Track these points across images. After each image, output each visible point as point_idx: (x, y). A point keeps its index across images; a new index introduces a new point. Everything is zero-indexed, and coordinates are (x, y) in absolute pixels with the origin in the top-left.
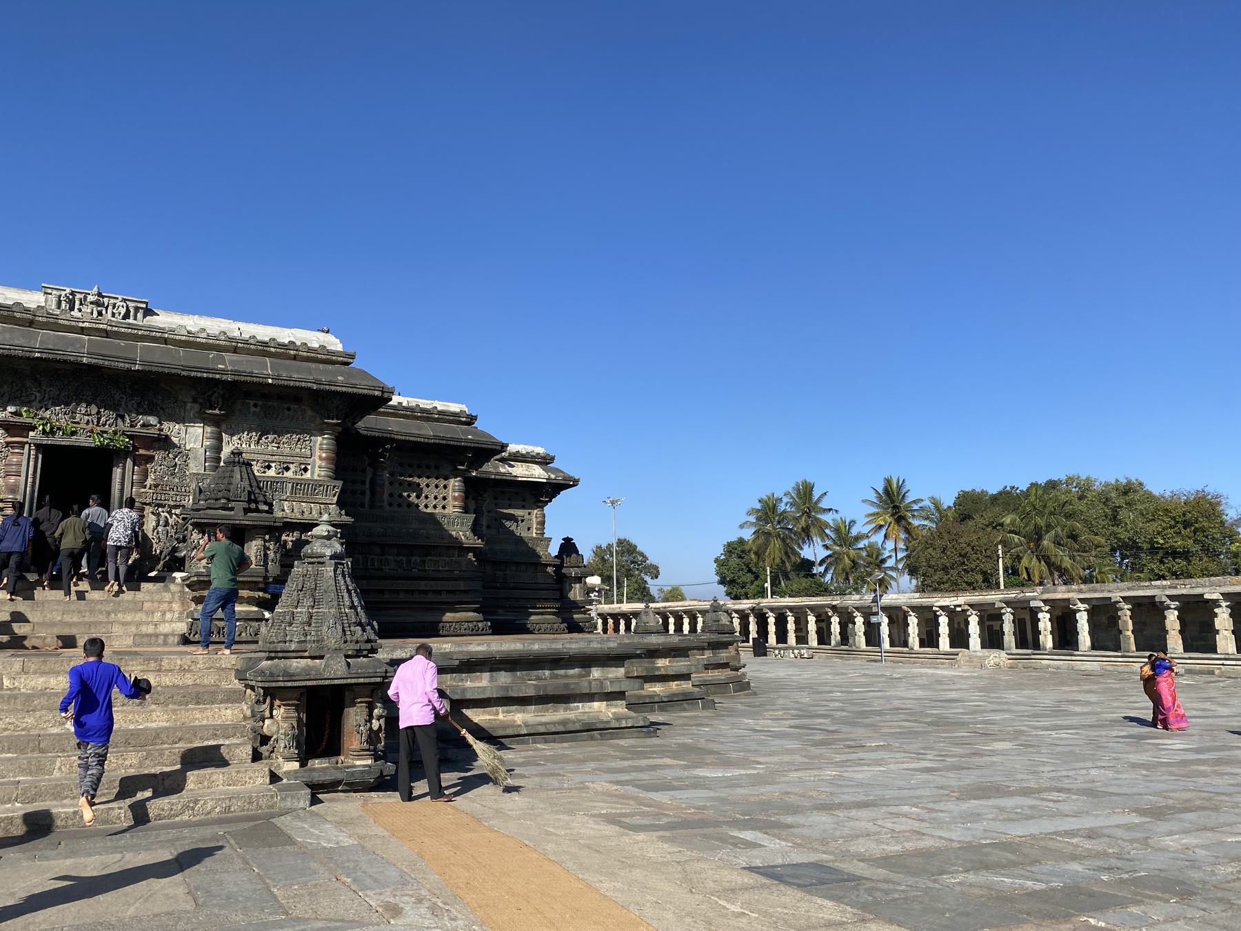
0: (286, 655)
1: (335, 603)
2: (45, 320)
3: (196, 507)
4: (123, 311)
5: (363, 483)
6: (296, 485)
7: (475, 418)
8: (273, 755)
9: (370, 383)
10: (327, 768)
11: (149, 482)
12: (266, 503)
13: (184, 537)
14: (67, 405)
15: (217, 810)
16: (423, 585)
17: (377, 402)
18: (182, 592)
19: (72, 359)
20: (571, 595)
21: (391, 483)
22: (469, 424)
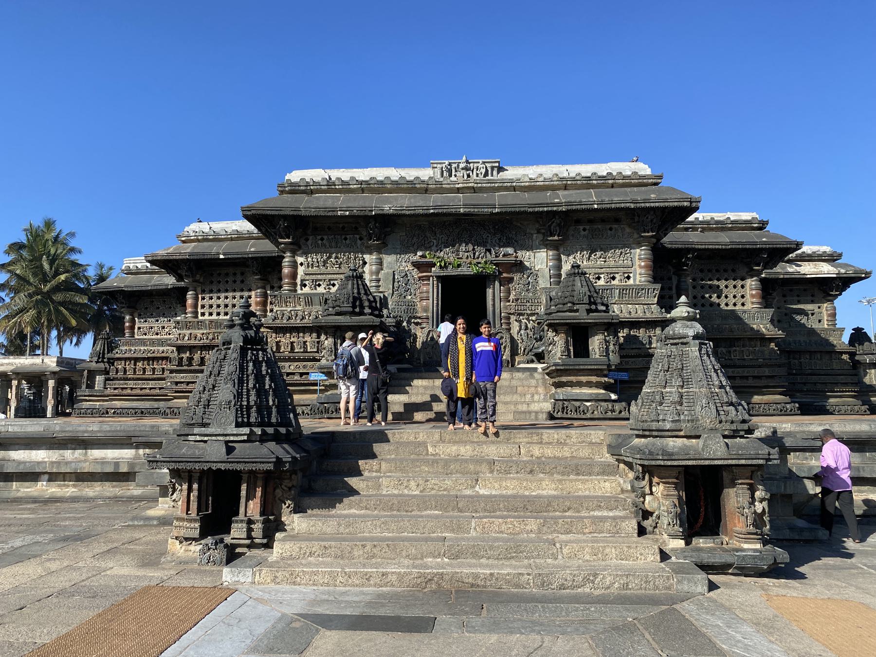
0: (660, 433)
1: (705, 383)
2: (434, 186)
3: (549, 311)
4: (483, 171)
5: (670, 289)
6: (623, 290)
7: (767, 223)
8: (657, 530)
9: (679, 196)
10: (714, 549)
11: (512, 297)
12: (603, 304)
13: (540, 337)
14: (453, 246)
15: (616, 585)
18: (543, 379)
19: (453, 210)
20: (867, 380)
21: (694, 287)
22: (760, 229)
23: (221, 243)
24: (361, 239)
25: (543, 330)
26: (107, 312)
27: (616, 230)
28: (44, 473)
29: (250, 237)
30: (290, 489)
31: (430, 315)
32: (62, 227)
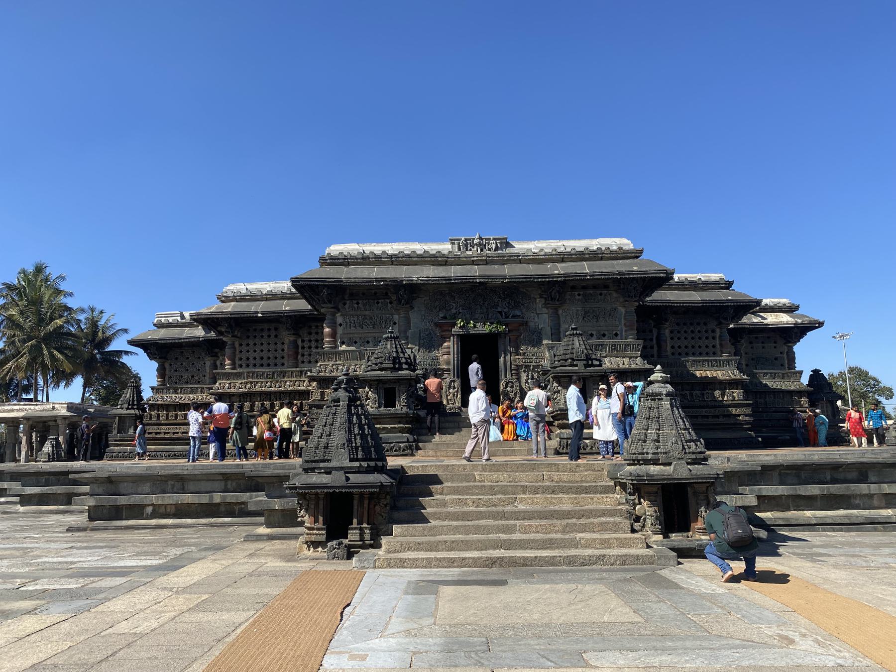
4: (494, 246)
5: (651, 340)
9: (657, 268)
12: (597, 360)
16: (704, 412)
17: (663, 280)
21: (672, 339)
22: (727, 288)
23: (257, 303)
24: (391, 303)
25: (549, 381)
26: (98, 356)
27: (605, 295)
28: (149, 505)
29: (283, 296)
30: (386, 506)
31: (451, 367)
32: (53, 271)
